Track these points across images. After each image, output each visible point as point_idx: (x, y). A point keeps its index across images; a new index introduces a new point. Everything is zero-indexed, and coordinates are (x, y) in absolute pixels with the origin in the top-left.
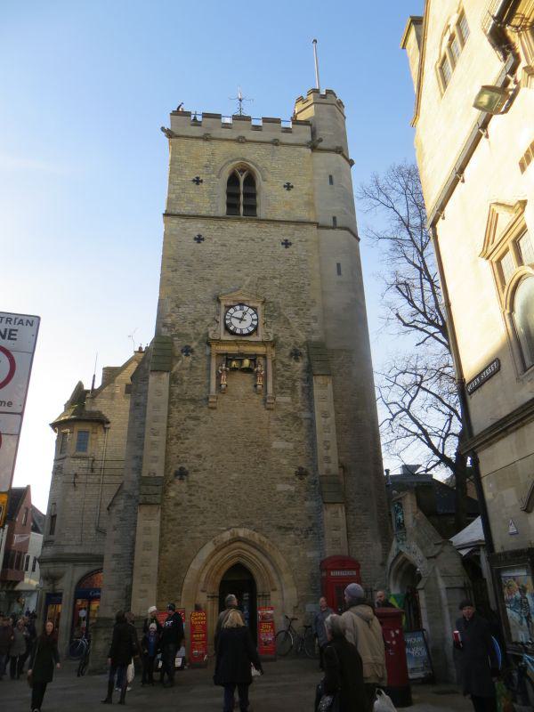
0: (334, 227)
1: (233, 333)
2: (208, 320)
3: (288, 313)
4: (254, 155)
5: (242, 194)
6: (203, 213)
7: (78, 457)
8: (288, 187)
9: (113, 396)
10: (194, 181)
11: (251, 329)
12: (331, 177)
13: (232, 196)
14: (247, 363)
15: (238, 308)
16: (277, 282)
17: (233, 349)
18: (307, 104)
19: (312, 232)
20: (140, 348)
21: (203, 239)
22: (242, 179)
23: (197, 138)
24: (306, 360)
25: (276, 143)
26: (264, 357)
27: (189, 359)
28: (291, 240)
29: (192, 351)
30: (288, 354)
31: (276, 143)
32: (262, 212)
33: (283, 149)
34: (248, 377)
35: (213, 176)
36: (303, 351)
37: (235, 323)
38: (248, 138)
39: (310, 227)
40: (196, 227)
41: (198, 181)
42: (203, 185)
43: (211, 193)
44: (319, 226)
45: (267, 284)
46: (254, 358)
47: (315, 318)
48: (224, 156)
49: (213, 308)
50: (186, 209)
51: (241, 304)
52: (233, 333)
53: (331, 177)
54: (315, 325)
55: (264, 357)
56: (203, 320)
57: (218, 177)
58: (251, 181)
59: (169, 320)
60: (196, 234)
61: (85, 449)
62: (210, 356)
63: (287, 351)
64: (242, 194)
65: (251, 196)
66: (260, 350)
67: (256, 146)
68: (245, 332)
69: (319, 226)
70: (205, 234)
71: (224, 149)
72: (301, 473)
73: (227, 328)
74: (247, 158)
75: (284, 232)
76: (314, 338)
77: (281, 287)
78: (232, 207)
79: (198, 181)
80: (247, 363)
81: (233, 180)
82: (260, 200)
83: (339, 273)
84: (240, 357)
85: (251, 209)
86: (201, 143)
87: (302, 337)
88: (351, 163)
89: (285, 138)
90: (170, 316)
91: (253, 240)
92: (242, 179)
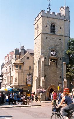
0: (67, 37)
3: (60, 52)
4: (55, 21)
5: (53, 28)
8: (61, 28)
12: (67, 27)
13: (51, 29)
14: (54, 60)
17: (52, 58)
18: (63, 9)
19: (64, 38)
23: (46, 17)
31: (59, 19)
33: (60, 20)
34: (54, 62)
39: (63, 37)
40: (46, 36)
41: (46, 26)
43: (48, 29)
44: (65, 36)
45: (57, 47)
46: (55, 60)
48: (51, 21)
49: (49, 50)
50: (45, 32)
51: (53, 51)
52: (52, 55)
58: (54, 26)
59: (43, 53)
61: (21, 68)
63: (59, 59)
64: (53, 28)
65: (54, 29)
66: (56, 58)
67: (56, 19)
69: (65, 36)
71: (51, 19)
72: (61, 77)
75: (58, 38)
77: (58, 47)
78: (51, 32)
79: (46, 26)
80: (54, 60)
81: (51, 26)
82: (56, 30)
84: (53, 60)
85: (54, 32)
86: (46, 18)
88: (70, 22)
89: (61, 18)
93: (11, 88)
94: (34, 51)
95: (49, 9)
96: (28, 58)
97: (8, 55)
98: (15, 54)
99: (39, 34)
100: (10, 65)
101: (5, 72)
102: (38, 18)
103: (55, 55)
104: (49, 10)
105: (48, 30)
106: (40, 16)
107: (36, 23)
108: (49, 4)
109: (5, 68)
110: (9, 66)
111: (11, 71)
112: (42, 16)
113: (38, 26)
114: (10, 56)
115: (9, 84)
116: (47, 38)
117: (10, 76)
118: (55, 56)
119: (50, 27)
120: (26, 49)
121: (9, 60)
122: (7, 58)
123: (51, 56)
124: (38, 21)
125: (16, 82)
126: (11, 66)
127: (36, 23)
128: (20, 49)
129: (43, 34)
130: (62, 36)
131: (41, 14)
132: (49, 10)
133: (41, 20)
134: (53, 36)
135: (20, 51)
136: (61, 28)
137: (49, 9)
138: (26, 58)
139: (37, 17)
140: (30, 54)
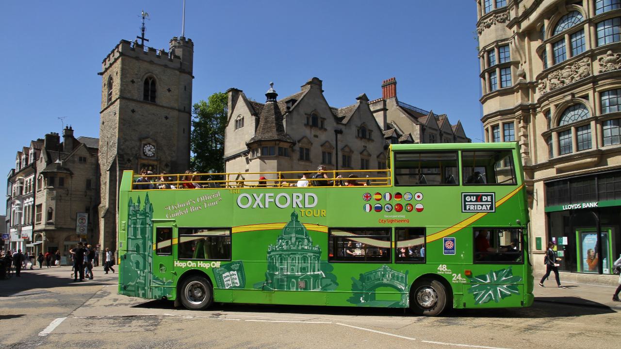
1: (146, 155)
2: (136, 149)
6: (135, 98)
7: (61, 188)
8: (169, 90)
9: (74, 162)
10: (131, 81)
11: (153, 155)
13: (146, 91)
15: (148, 145)
16: (162, 134)
20: (67, 127)
21: (135, 111)
22: (150, 82)
24: (170, 168)
25: (166, 66)
26: (156, 166)
27: (130, 164)
28: (168, 116)
29: (131, 161)
30: (164, 165)
31: (166, 66)
32: (158, 101)
35: (139, 80)
36: (170, 165)
37: (147, 151)
38: (155, 62)
40: (132, 105)
41: (133, 82)
42: (135, 85)
47: (174, 151)
49: (138, 144)
50: (128, 95)
53: (185, 87)
54: (174, 154)
55: (156, 166)
56: (134, 148)
57: (142, 80)
58: (154, 83)
59: (122, 147)
60: (132, 108)
62: (137, 164)
63: (164, 163)
65: (154, 91)
66: (155, 163)
68: (151, 156)
70: (136, 109)
71: (146, 66)
73: (144, 153)
74: (154, 72)
76: (174, 159)
78: (146, 96)
83: (184, 133)
85: (153, 98)
87: (169, 158)
88: (193, 77)
90: (122, 145)
91: (154, 114)
92: (150, 82)
93: (35, 235)
94: (100, 143)
95: (143, 39)
96: (83, 160)
97: (26, 149)
98: (47, 148)
99: (113, 100)
100: (34, 176)
101: (18, 193)
102: (112, 60)
103: (154, 156)
104: (143, 42)
105: (137, 92)
106: (117, 55)
107: (107, 69)
108: (142, 27)
109: (16, 185)
110: (28, 179)
111: (34, 192)
112: (121, 54)
113: (111, 79)
114: (32, 151)
115: (29, 225)
116: (133, 111)
117: (34, 205)
118: (153, 158)
119: (142, 83)
120: (76, 135)
121: (31, 160)
122: (24, 157)
123: (145, 157)
124: (111, 65)
125: (51, 221)
126: (35, 178)
127: (107, 69)
128: (61, 135)
129: (124, 101)
130: (172, 109)
131: (120, 50)
132: (143, 42)
133: (118, 65)
134: (148, 107)
135: (62, 140)
136: (169, 90)
137: (143, 39)
138: (76, 159)
139: (109, 56)
140: (90, 148)
